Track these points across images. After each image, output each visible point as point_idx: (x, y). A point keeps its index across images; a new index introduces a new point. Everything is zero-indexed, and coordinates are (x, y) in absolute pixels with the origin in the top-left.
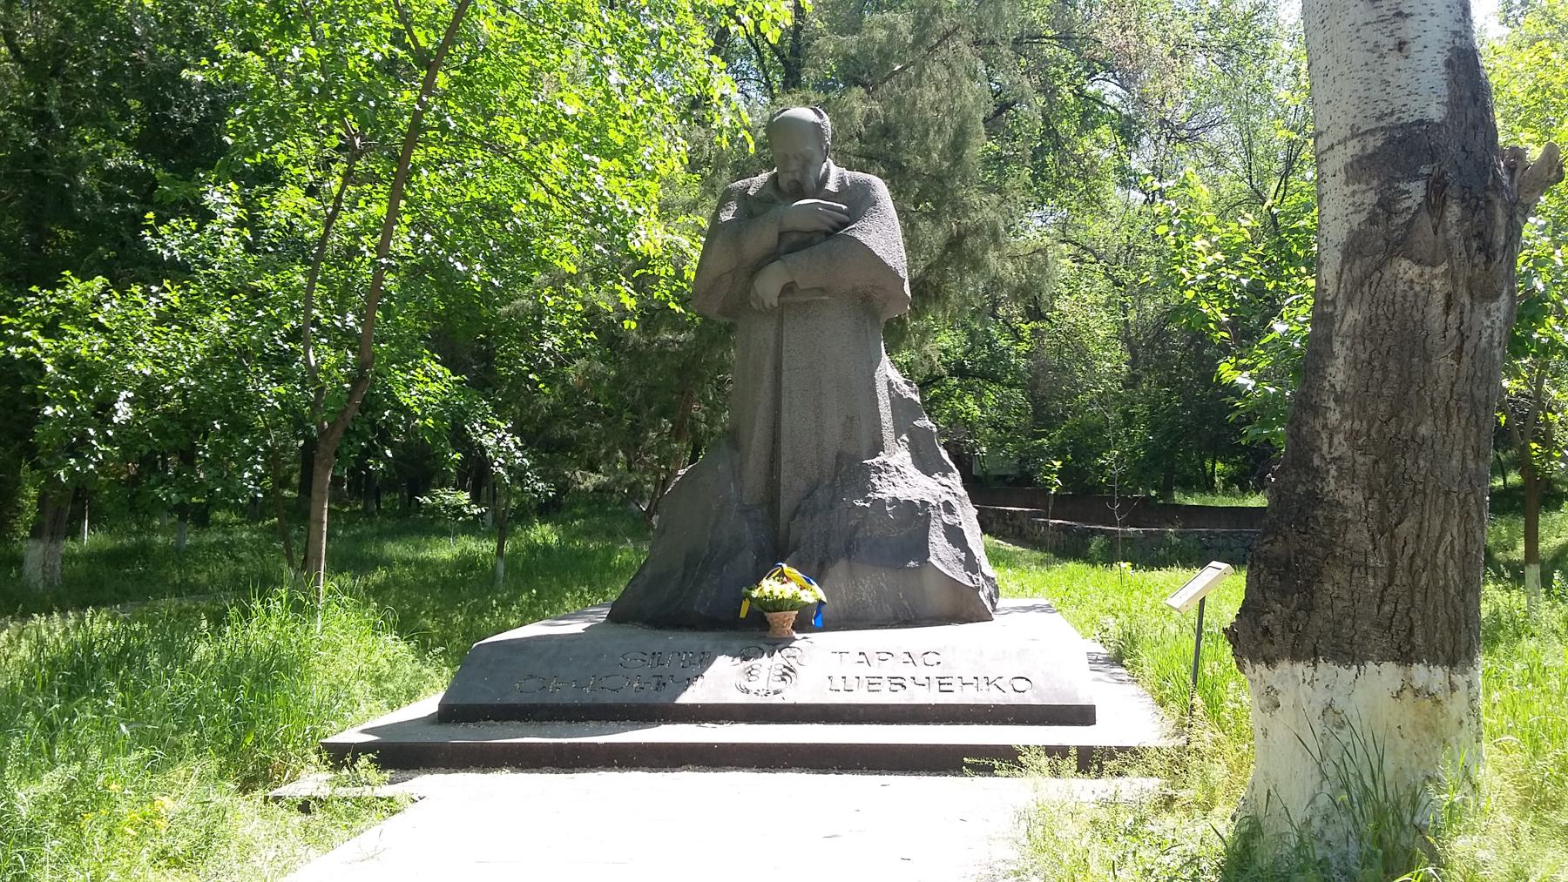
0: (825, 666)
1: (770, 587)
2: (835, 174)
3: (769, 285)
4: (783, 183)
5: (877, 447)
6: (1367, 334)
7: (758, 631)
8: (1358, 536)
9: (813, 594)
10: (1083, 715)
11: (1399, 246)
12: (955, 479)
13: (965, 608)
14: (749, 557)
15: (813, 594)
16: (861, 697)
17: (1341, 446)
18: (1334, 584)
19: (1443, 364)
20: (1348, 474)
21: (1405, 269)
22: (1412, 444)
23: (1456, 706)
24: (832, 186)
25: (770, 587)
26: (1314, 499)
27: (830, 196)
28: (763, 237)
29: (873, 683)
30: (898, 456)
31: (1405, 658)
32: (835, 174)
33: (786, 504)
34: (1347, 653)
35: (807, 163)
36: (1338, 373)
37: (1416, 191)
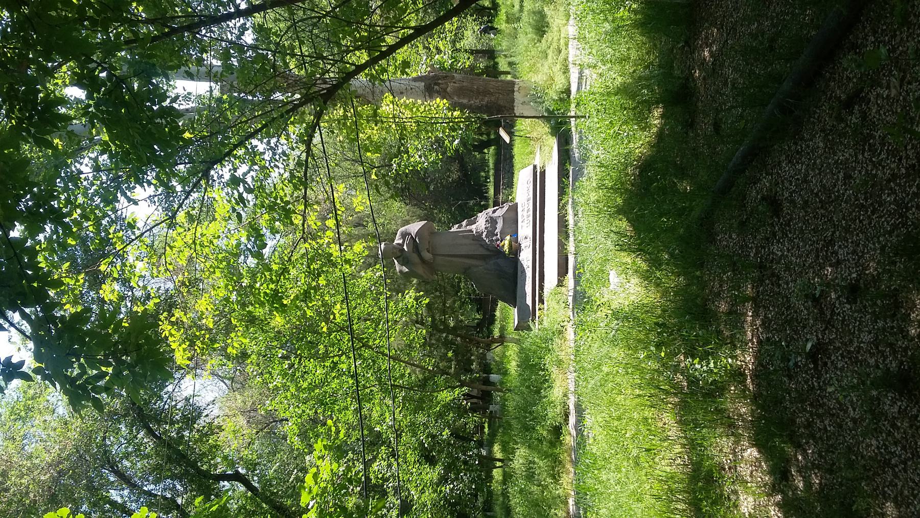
0: (525, 230)
1: (506, 248)
2: (398, 241)
3: (427, 256)
4: (399, 254)
5: (471, 231)
6: (459, 97)
7: (516, 250)
8: (493, 98)
9: (508, 238)
10: (535, 167)
11: (445, 90)
12: (480, 215)
13: (514, 209)
14: (500, 261)
15: (508, 238)
16: (531, 218)
17: (478, 101)
18: (501, 103)
19: (465, 84)
20: (482, 100)
21: (449, 89)
22: (478, 89)
23: (521, 84)
24: (401, 242)
25: (506, 248)
26: (486, 106)
27: (404, 242)
28: (415, 258)
29: (528, 216)
30: (473, 227)
31: (513, 91)
32: (398, 241)
33: (485, 252)
34: (513, 101)
35: (394, 247)
36: (465, 101)
37: (436, 87)
